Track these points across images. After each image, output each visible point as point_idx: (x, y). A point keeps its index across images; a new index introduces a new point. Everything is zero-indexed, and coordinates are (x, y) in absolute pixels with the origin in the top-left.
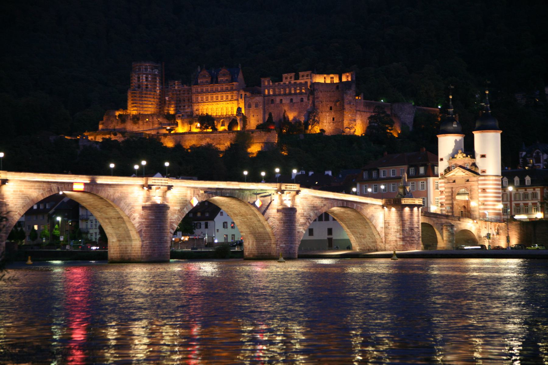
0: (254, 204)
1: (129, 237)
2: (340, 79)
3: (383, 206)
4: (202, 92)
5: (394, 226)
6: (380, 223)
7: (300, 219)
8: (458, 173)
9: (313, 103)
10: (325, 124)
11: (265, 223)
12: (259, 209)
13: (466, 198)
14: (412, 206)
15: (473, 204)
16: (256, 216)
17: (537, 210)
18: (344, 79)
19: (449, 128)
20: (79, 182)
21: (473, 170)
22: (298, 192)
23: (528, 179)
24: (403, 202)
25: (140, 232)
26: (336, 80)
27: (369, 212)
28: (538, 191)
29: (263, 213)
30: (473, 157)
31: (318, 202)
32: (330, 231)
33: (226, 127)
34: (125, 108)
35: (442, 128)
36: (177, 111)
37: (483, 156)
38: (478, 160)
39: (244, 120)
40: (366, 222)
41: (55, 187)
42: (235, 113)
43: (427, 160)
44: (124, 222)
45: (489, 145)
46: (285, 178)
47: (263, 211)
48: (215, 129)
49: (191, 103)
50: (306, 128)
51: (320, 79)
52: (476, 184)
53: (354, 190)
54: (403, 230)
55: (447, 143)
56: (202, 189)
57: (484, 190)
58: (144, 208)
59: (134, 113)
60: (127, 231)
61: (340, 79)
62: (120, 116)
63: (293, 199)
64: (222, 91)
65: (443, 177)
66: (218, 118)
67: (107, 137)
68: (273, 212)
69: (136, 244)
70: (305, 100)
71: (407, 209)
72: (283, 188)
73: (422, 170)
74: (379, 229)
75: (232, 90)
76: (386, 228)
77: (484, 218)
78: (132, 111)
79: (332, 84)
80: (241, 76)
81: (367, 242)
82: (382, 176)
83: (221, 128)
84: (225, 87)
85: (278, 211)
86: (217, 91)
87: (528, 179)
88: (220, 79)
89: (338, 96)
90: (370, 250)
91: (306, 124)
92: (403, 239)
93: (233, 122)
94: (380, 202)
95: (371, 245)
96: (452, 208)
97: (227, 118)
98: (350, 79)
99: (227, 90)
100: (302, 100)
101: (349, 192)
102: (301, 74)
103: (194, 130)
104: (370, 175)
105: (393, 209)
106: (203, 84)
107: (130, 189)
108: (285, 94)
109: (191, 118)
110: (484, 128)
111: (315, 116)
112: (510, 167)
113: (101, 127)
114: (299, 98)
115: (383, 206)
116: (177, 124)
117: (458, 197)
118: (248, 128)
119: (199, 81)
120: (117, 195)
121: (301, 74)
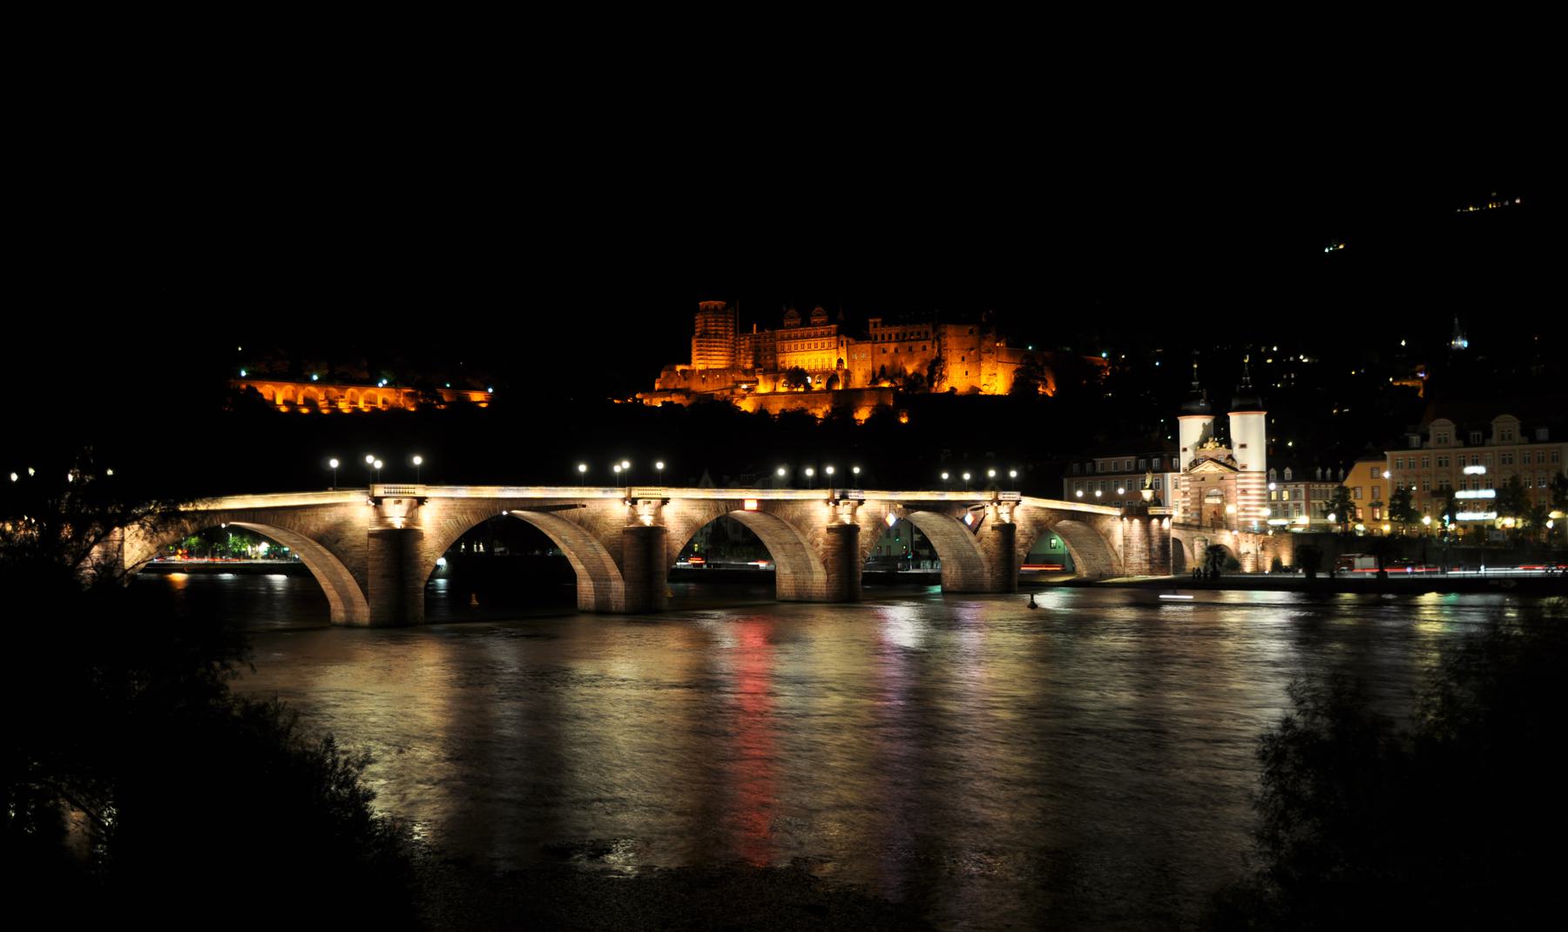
0: (963, 520)
1: (809, 569)
3: (1122, 518)
4: (789, 338)
5: (1137, 543)
6: (1118, 540)
7: (1020, 539)
8: (1209, 468)
11: (977, 545)
12: (969, 527)
13: (1218, 501)
14: (1161, 518)
15: (1230, 510)
16: (963, 535)
17: (1300, 513)
19: (1195, 407)
20: (751, 499)
21: (1230, 464)
22: (1018, 503)
23: (1288, 471)
24: (1152, 511)
25: (824, 563)
27: (1106, 525)
28: (1302, 487)
29: (975, 532)
30: (1229, 447)
31: (1041, 515)
33: (823, 386)
34: (688, 362)
35: (1185, 407)
36: (757, 364)
37: (1243, 446)
38: (1236, 451)
39: (848, 373)
40: (1103, 538)
41: (722, 506)
42: (834, 366)
43: (1164, 452)
44: (803, 549)
45: (1249, 429)
46: (1004, 485)
47: (975, 528)
48: (808, 387)
49: (774, 353)
50: (931, 385)
52: (1235, 483)
53: (1080, 494)
54: (1150, 550)
55: (1192, 428)
56: (900, 502)
57: (1244, 492)
58: (829, 530)
59: (701, 367)
60: (807, 561)
62: (683, 372)
63: (1011, 513)
64: (816, 336)
65: (1187, 472)
66: (813, 374)
67: (668, 399)
68: (986, 529)
69: (819, 577)
71: (1155, 522)
72: (1001, 497)
73: (1156, 461)
74: (1116, 548)
75: (829, 335)
76: (1126, 546)
77: (1245, 528)
78: (698, 364)
80: (840, 316)
81: (1100, 564)
82: (1099, 469)
83: (817, 387)
84: (820, 330)
85: (993, 528)
86: (809, 337)
87: (1288, 471)
90: (1102, 576)
91: (931, 380)
92: (1150, 562)
93: (832, 378)
94: (1117, 512)
95: (1104, 570)
96: (1200, 514)
97: (824, 373)
99: (823, 335)
100: (924, 348)
101: (1074, 499)
103: (782, 389)
104: (1082, 467)
105: (1136, 522)
106: (790, 327)
107: (812, 506)
109: (774, 372)
110: (1242, 409)
112: (1277, 460)
113: (657, 386)
115: (1122, 518)
116: (757, 382)
117: (1208, 501)
118: (851, 386)
119: (786, 323)
120: (797, 514)
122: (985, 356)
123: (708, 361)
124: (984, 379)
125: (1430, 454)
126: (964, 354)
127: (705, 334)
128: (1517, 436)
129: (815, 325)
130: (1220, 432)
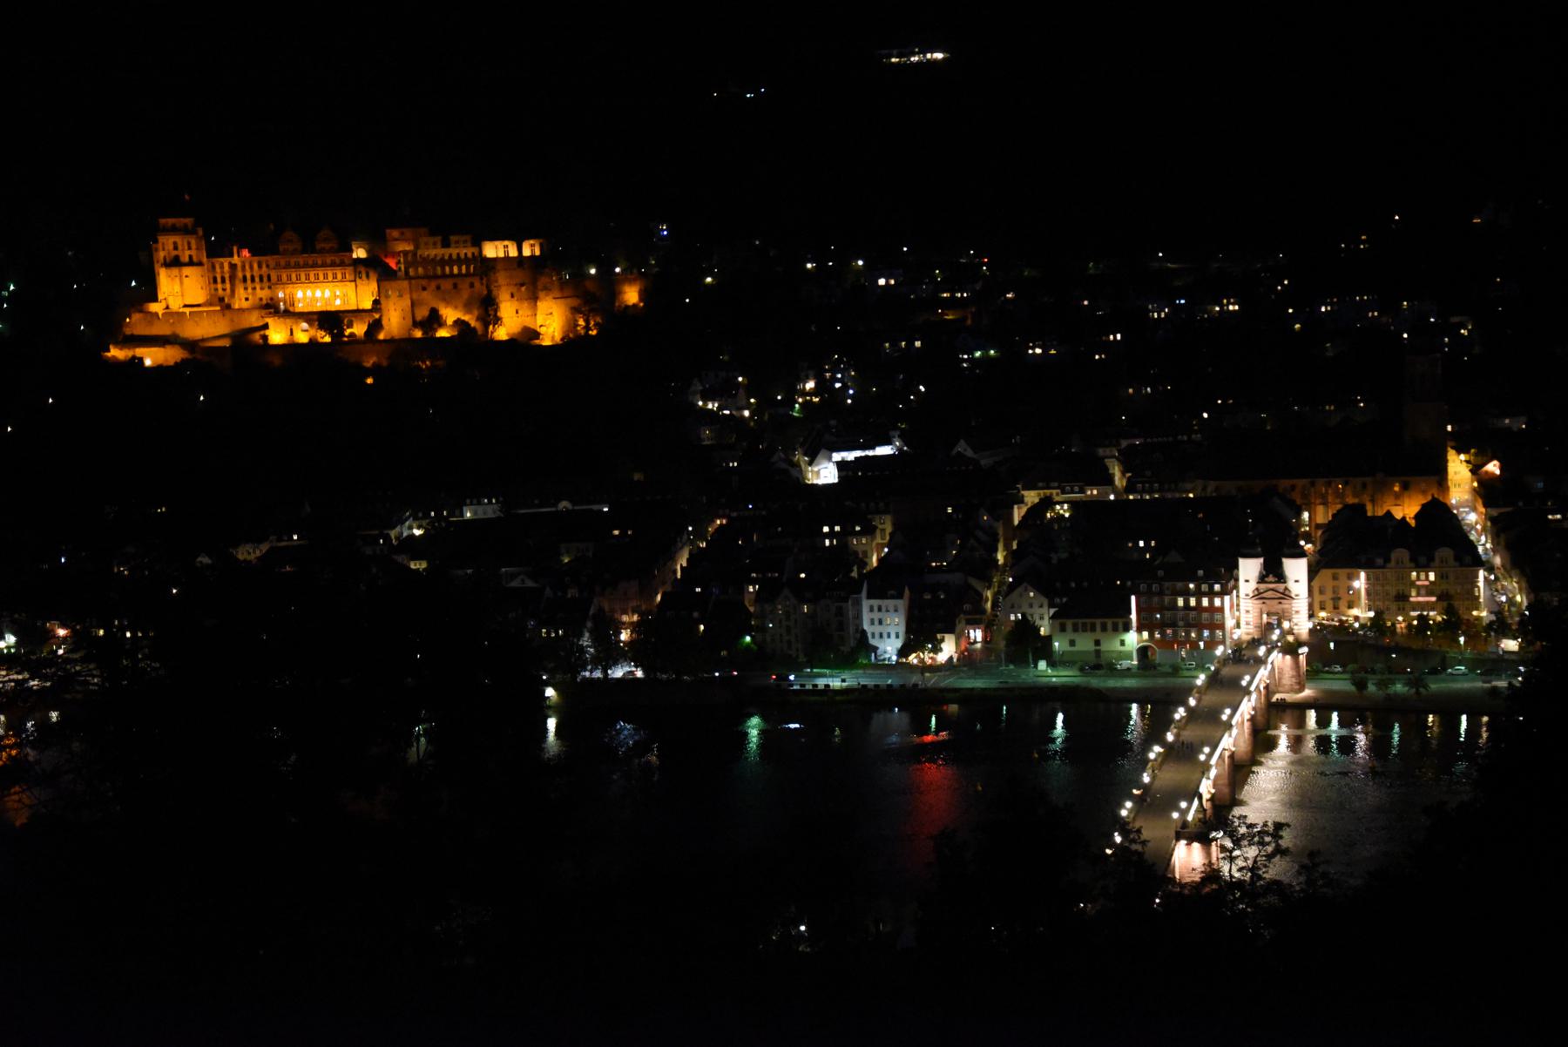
2: (520, 249)
4: (287, 266)
9: (488, 287)
10: (510, 321)
18: (527, 252)
26: (513, 253)
32: (1097, 643)
38: (1291, 585)
51: (492, 250)
55: (1249, 569)
61: (520, 249)
64: (324, 265)
70: (477, 284)
73: (1217, 587)
79: (507, 258)
88: (319, 246)
89: (532, 279)
98: (537, 253)
99: (333, 265)
100: (472, 285)
102: (453, 238)
105: (1288, 657)
108: (444, 276)
111: (496, 311)
114: (468, 280)
121: (453, 238)
122: (541, 294)
123: (179, 291)
124: (540, 320)
125: (1389, 573)
126: (514, 290)
127: (174, 263)
128: (1451, 561)
129: (322, 251)
130: (1273, 572)
